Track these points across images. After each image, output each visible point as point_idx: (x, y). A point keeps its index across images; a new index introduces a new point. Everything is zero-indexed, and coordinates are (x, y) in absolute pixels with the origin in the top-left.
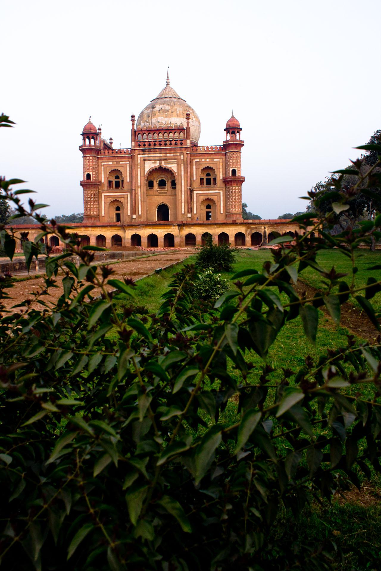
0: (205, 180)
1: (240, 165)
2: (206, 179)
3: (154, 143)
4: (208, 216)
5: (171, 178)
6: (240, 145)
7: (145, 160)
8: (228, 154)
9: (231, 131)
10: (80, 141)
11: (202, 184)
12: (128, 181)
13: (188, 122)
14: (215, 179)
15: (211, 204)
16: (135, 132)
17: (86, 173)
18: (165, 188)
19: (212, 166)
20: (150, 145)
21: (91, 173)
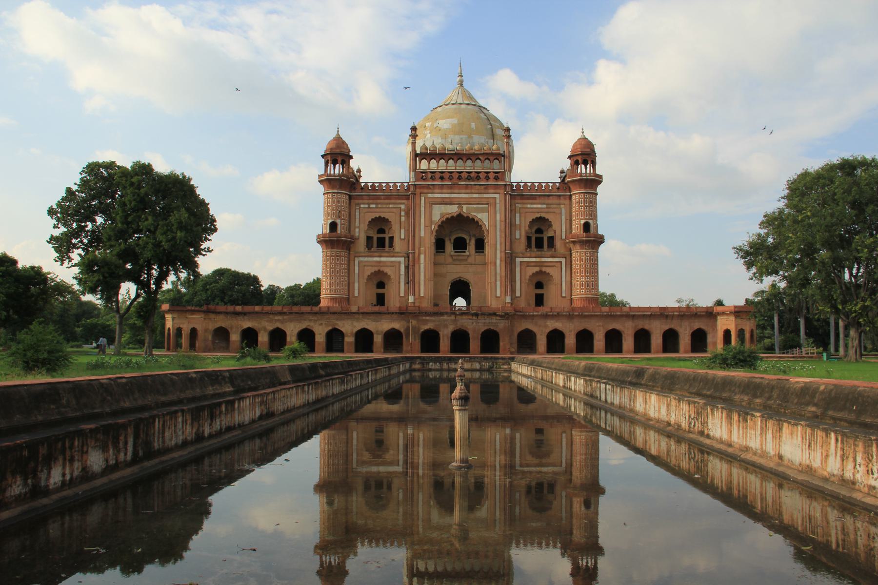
0: (533, 239)
1: (596, 216)
5: (474, 236)
8: (573, 197)
9: (580, 159)
10: (318, 167)
11: (529, 246)
12: (403, 237)
14: (551, 239)
16: (417, 155)
17: (330, 221)
19: (547, 216)
21: (338, 221)
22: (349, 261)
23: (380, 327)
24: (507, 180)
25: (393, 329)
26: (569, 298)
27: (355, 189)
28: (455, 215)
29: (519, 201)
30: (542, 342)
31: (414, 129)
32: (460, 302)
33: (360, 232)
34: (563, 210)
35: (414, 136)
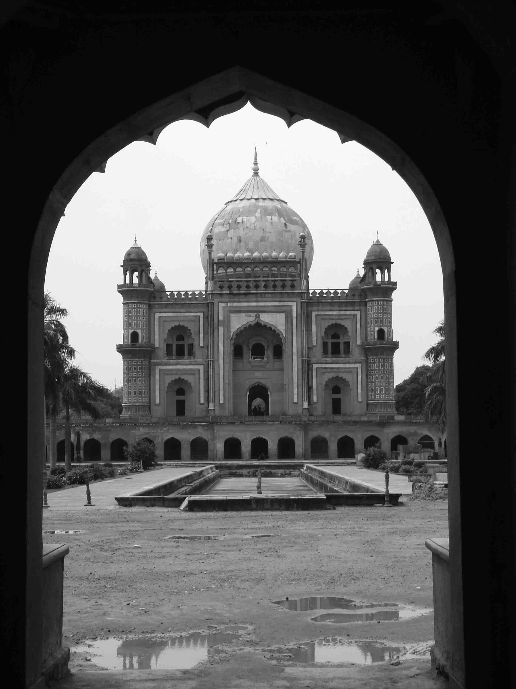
1: (390, 322)
2: (333, 344)
3: (245, 284)
4: (337, 407)
6: (389, 288)
7: (230, 313)
11: (325, 352)
12: (202, 344)
13: (303, 252)
14: (347, 344)
15: (341, 386)
16: (214, 263)
17: (131, 331)
18: (262, 358)
19: (342, 322)
20: (239, 287)
21: (139, 331)
22: (150, 369)
23: (185, 437)
24: (304, 288)
25: (199, 437)
26: (365, 400)
27: (154, 297)
28: (253, 324)
29: (315, 308)
30: (333, 447)
31: (209, 238)
32: (258, 401)
33: (159, 340)
34: (358, 317)
35: (210, 246)
